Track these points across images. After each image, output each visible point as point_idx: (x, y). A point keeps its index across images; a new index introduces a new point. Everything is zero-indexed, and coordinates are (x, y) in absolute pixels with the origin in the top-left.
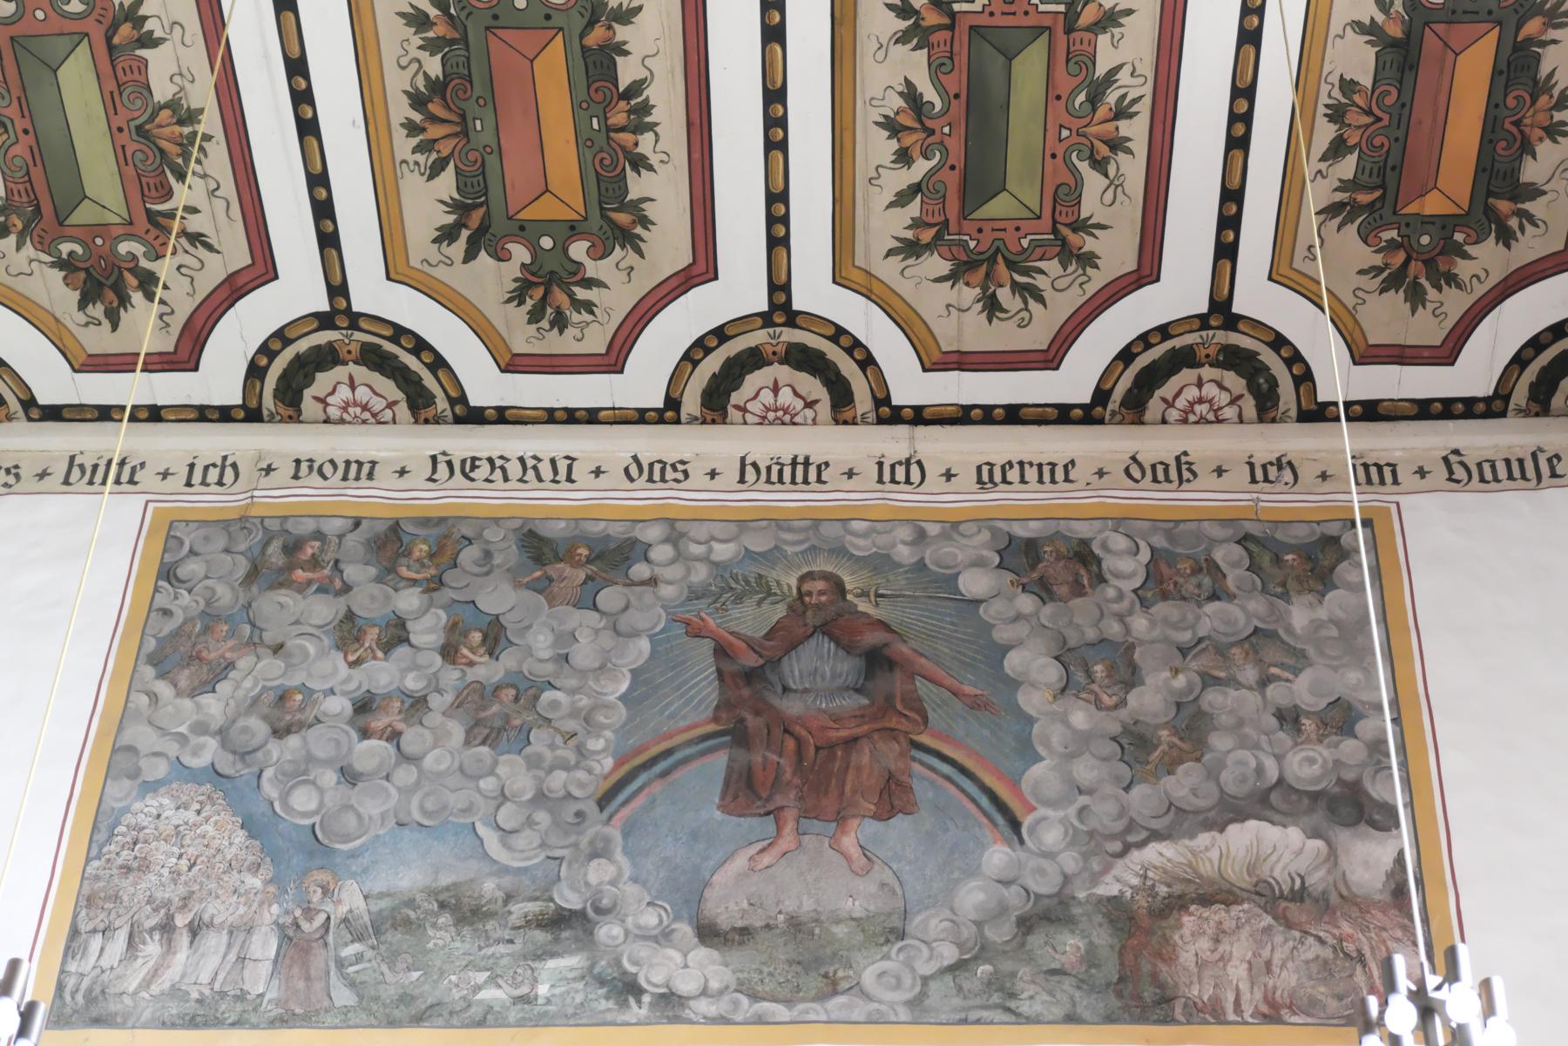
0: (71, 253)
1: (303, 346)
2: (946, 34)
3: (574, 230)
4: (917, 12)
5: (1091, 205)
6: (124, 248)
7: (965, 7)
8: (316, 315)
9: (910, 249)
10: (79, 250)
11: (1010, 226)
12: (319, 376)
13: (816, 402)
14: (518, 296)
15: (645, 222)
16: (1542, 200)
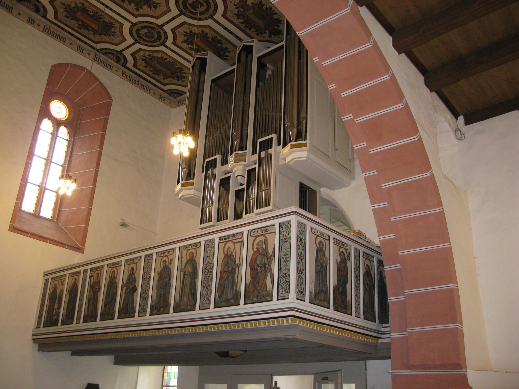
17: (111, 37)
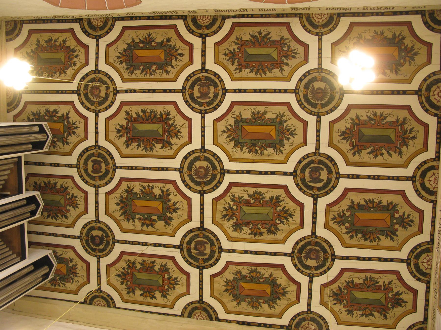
0: (391, 305)
1: (414, 270)
2: (359, 146)
3: (393, 216)
4: (355, 152)
5: (393, 119)
6: (390, 296)
7: (355, 143)
8: (407, 266)
9: (400, 153)
10: (390, 304)
11: (397, 134)
12: (421, 268)
13: (433, 173)
14: (406, 228)
15: (392, 203)
16: (396, 33)
17: (119, 52)
